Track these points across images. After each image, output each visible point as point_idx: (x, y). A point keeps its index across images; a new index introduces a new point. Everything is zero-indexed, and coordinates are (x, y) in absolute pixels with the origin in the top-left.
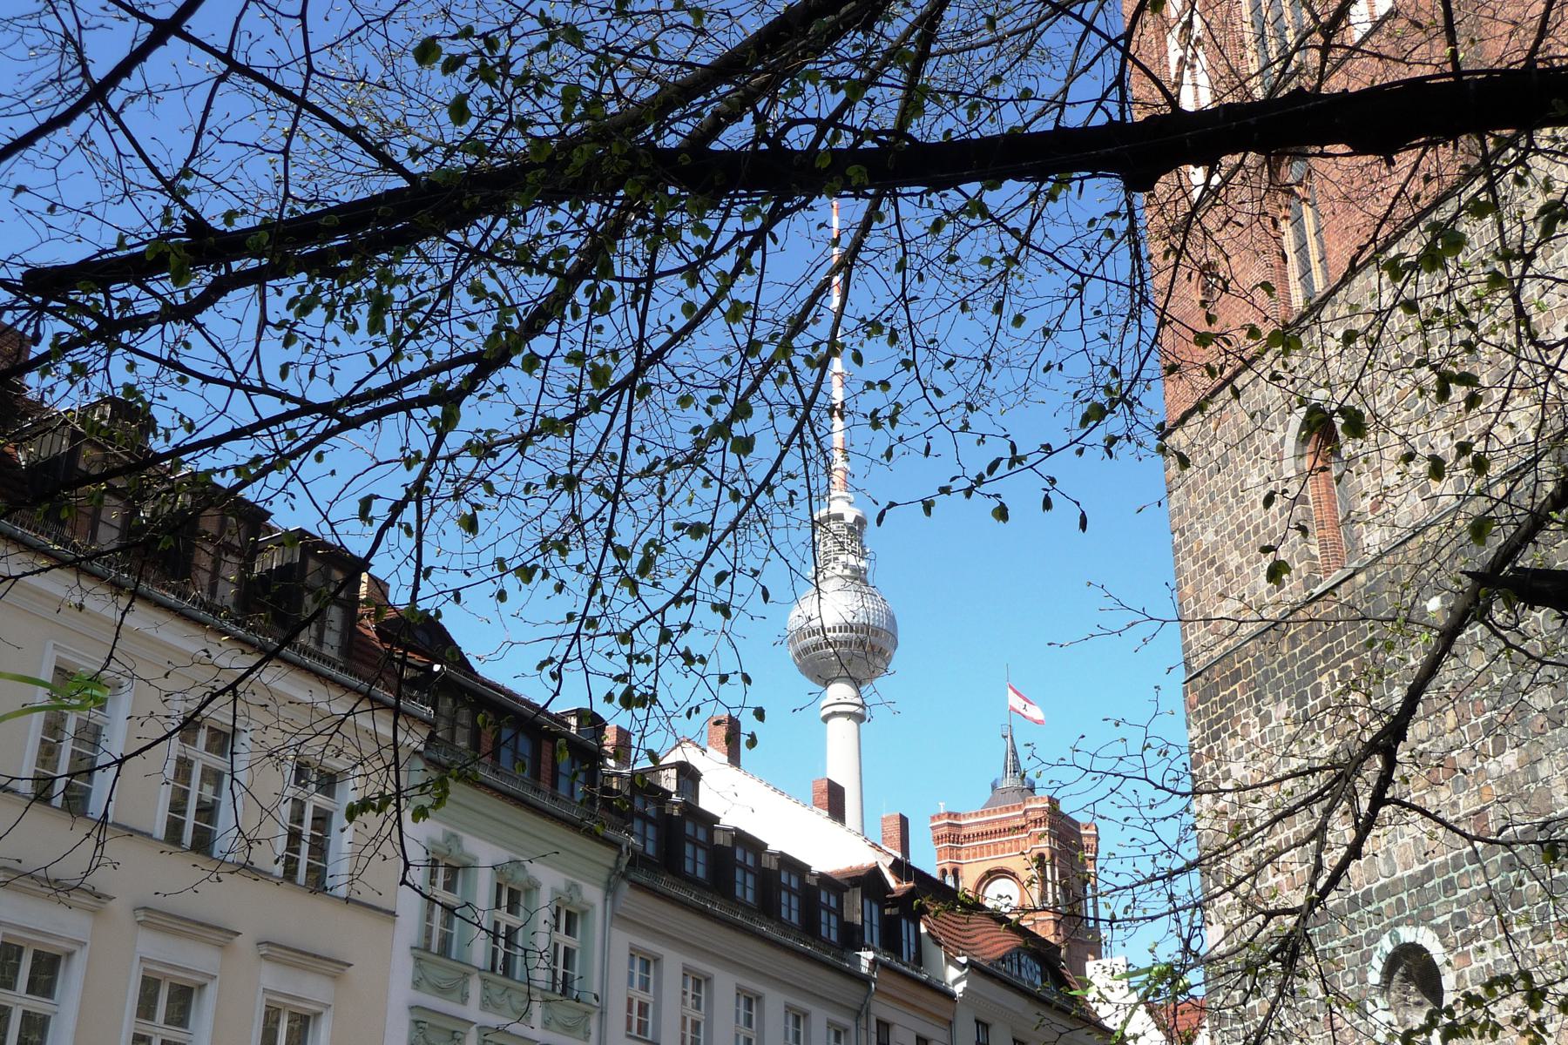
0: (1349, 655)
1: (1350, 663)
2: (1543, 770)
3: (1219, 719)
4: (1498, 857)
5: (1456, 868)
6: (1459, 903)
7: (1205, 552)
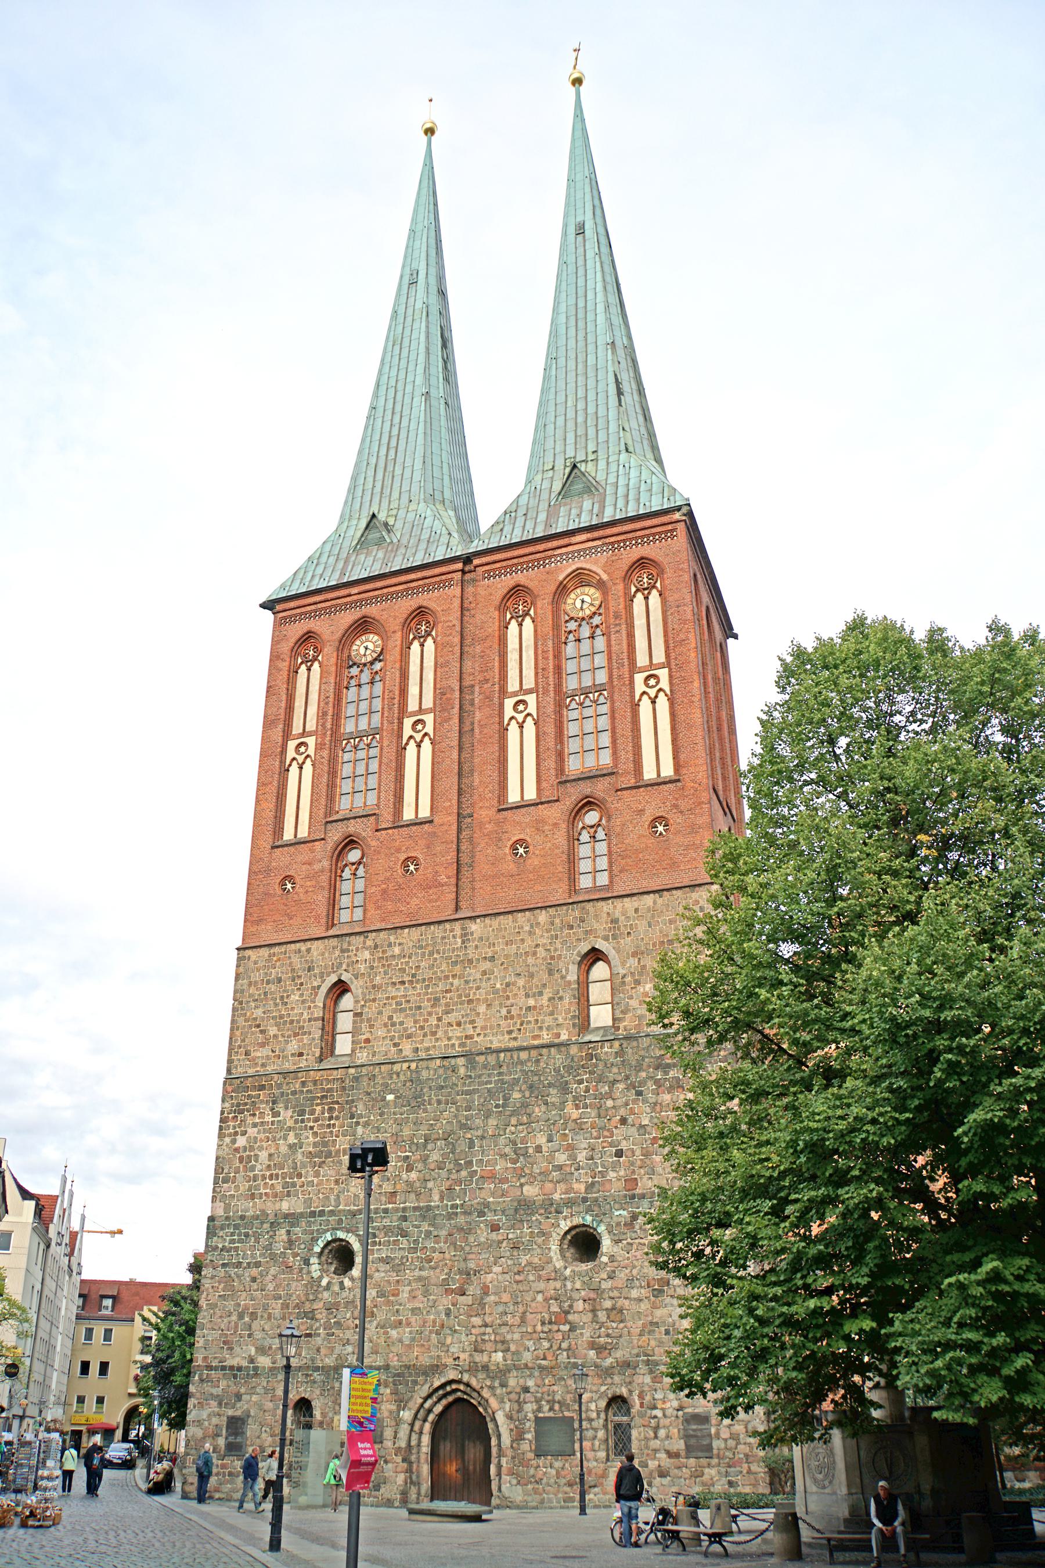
0: (337, 1103)
1: (336, 1106)
2: (430, 1185)
3: (246, 1104)
7: (255, 1019)
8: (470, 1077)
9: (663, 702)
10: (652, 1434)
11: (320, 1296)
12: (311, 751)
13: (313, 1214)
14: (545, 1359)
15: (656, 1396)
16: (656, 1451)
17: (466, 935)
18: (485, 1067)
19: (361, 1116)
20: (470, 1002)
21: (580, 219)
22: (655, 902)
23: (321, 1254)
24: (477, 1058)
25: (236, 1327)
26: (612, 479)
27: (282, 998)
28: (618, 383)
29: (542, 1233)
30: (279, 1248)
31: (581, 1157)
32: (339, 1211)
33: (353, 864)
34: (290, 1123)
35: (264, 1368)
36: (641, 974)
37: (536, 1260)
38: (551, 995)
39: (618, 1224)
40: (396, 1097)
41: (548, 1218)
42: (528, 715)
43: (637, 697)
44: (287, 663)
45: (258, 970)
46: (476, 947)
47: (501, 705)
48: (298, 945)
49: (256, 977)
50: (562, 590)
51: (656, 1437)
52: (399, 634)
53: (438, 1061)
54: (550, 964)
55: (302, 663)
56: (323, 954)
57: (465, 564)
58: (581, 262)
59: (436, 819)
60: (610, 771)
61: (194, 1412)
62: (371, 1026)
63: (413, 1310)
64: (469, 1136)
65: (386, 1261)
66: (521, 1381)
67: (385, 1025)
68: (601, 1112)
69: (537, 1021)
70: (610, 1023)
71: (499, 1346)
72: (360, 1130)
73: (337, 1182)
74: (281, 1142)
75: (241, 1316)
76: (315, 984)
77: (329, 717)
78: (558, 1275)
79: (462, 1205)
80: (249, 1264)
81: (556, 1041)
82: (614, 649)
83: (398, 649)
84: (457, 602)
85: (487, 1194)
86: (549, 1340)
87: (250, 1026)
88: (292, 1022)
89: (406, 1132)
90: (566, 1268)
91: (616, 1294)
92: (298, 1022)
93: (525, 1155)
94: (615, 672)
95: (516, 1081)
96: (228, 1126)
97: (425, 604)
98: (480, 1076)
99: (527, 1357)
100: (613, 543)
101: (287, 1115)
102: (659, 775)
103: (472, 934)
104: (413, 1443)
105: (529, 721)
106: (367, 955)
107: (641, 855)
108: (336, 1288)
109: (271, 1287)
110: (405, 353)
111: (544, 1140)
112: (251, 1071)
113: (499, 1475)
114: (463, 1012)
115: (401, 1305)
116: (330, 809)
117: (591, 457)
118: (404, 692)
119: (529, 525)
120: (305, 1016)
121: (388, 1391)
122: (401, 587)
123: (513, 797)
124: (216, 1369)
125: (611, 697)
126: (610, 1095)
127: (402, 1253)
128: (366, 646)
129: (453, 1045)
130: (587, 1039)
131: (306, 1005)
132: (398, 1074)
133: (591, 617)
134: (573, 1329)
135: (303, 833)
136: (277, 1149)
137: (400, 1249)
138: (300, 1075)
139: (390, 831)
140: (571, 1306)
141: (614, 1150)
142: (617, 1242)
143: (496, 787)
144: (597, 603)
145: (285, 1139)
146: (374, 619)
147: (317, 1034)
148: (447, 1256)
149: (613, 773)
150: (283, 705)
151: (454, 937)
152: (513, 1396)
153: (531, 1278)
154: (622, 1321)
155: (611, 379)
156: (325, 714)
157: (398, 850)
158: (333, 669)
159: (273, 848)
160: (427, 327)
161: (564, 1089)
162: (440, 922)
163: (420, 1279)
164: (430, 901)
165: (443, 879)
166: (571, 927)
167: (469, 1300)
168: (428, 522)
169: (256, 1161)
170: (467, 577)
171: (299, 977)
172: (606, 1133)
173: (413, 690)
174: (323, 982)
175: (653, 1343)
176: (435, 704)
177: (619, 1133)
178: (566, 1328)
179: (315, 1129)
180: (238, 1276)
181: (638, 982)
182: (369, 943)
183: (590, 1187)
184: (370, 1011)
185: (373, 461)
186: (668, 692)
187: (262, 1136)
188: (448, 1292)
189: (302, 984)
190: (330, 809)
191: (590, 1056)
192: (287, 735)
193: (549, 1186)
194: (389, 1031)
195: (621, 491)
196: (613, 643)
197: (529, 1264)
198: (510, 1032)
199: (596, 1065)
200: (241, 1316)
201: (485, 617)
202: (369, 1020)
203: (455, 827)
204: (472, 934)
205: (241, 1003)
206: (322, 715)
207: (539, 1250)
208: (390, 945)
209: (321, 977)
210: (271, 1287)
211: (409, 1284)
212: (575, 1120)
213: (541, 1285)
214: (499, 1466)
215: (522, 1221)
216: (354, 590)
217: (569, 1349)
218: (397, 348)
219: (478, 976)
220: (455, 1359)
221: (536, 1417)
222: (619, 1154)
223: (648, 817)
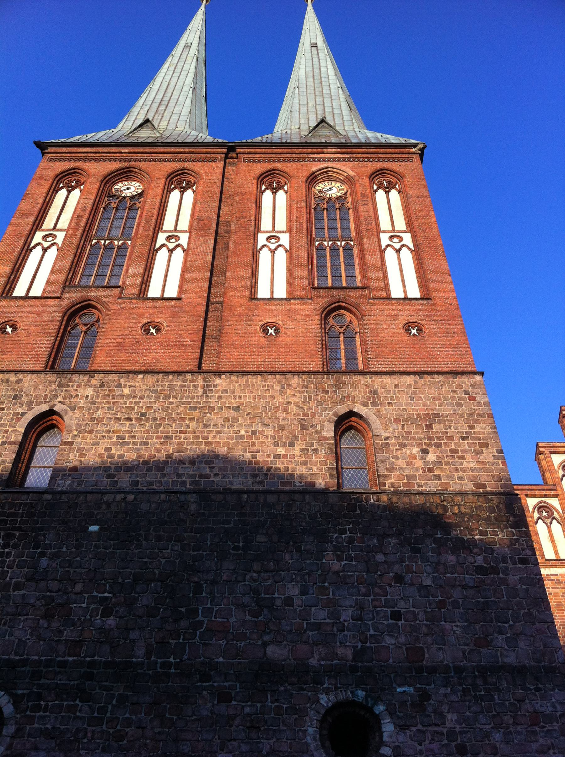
0: (19, 529)
2: (134, 635)
4: (82, 670)
8: (203, 514)
19: (49, 546)
22: (415, 381)
24: (213, 497)
31: (346, 615)
38: (304, 447)
40: (100, 529)
41: (303, 690)
46: (220, 397)
48: (7, 376)
50: (312, 179)
52: (162, 181)
53: (163, 496)
54: (302, 419)
56: (36, 386)
59: (184, 298)
64: (196, 579)
72: (44, 562)
76: (20, 411)
77: (84, 220)
94: (364, 228)
103: (216, 386)
105: (281, 251)
107: (396, 347)
111: (296, 591)
128: (130, 188)
129: (184, 483)
137: (76, 718)
139: (134, 301)
141: (389, 610)
157: (141, 315)
164: (170, 357)
166: (327, 392)
172: (377, 590)
174: (30, 409)
176: (191, 226)
181: (403, 445)
182: (93, 382)
183: (359, 654)
204: (216, 386)
208: (119, 386)
212: (337, 573)
216: (126, 150)
219: (220, 422)
222: (396, 616)
223: (402, 319)
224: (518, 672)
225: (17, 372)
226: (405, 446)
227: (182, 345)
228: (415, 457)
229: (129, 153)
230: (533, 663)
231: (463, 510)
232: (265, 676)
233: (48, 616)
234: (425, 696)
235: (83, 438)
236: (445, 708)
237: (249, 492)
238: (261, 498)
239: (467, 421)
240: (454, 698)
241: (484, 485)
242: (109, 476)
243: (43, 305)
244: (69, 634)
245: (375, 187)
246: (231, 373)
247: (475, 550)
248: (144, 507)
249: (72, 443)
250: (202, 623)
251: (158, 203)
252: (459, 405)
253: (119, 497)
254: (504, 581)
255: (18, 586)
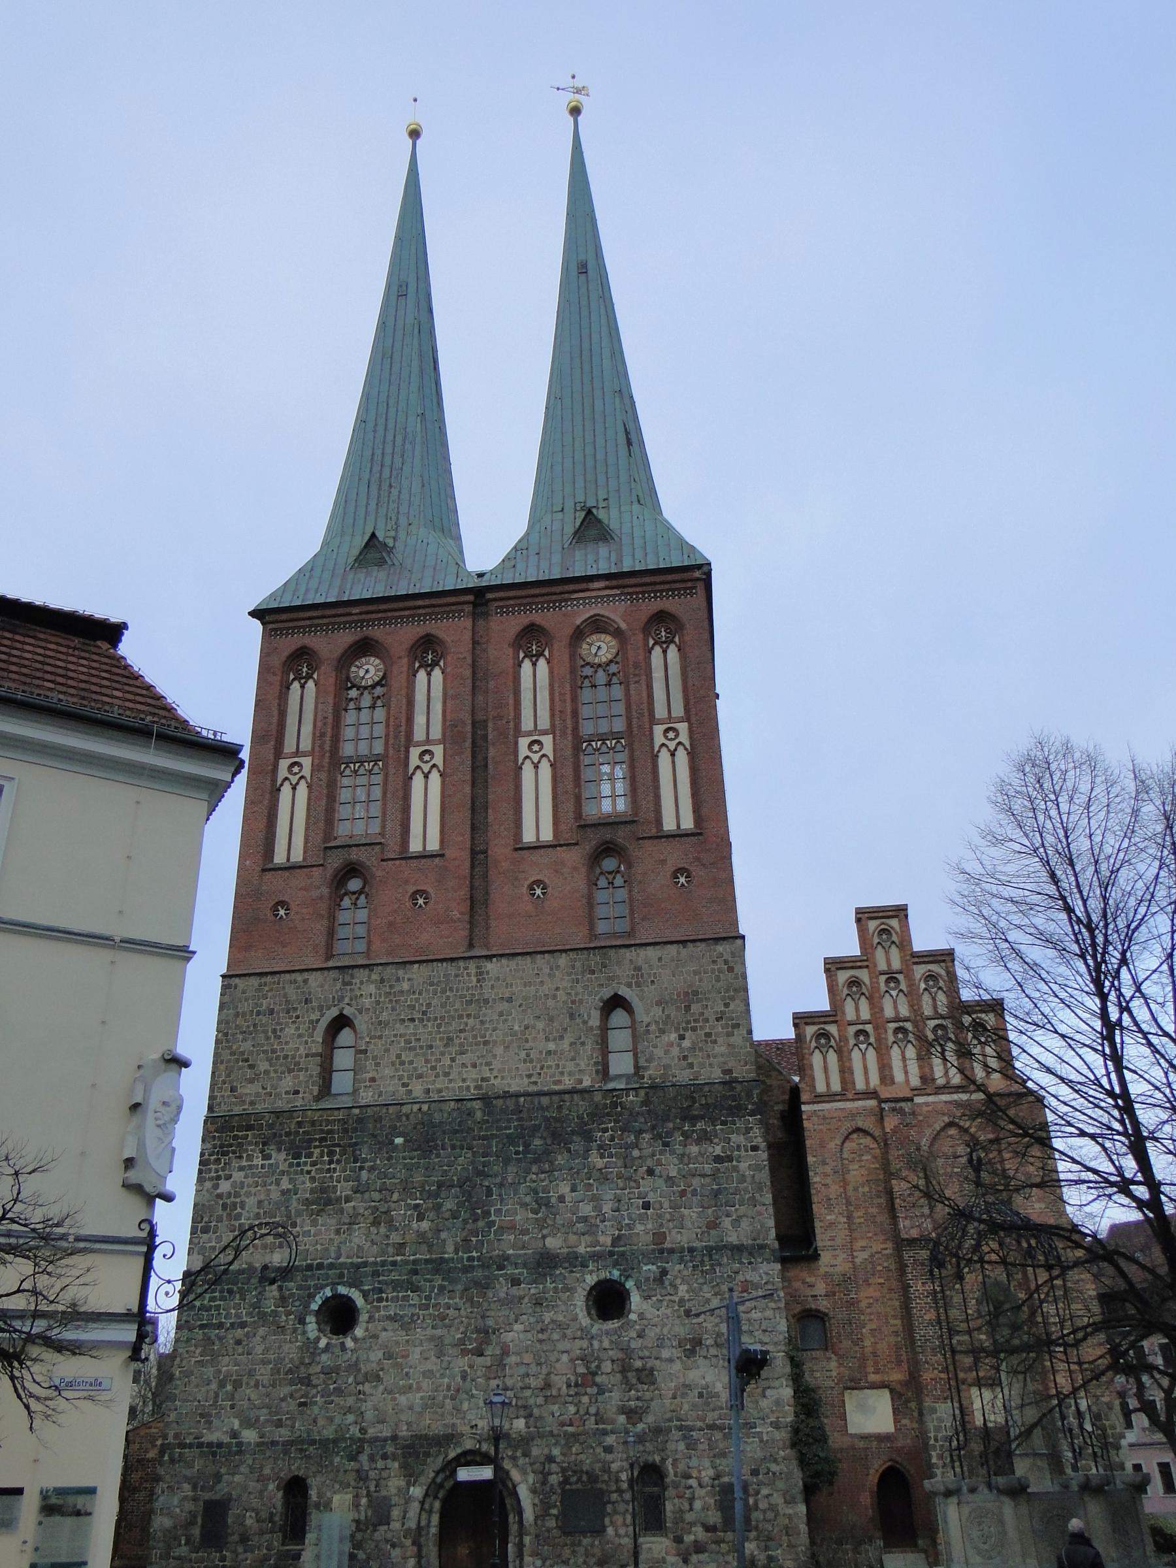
0: (339, 1145)
2: (443, 1235)
5: (383, 1266)
6: (379, 1282)
7: (243, 1053)
8: (487, 1121)
9: (682, 757)
10: (686, 1506)
11: (317, 1359)
12: (307, 771)
13: (309, 1267)
14: (571, 1425)
15: (691, 1465)
16: (692, 1524)
17: (481, 973)
18: (503, 1111)
19: (365, 1160)
20: (486, 1043)
21: (582, 257)
22: (679, 953)
23: (318, 1313)
25: (216, 1395)
26: (626, 528)
27: (274, 1031)
28: (627, 433)
29: (566, 1289)
30: (270, 1306)
31: (607, 1208)
32: (341, 1264)
33: (354, 893)
34: (283, 1167)
35: (249, 1443)
36: (665, 1023)
37: (560, 1318)
39: (647, 1279)
42: (544, 755)
43: (656, 749)
44: (279, 678)
45: (246, 1000)
47: (516, 743)
48: (294, 976)
49: (245, 1007)
50: (578, 635)
51: (691, 1509)
52: (405, 660)
53: (452, 1103)
55: (294, 679)
57: (476, 597)
58: (584, 303)
59: (447, 852)
60: (630, 819)
61: (161, 1498)
62: (377, 1065)
63: (424, 1373)
65: (393, 1319)
66: (546, 1451)
67: (393, 1064)
68: (627, 1162)
69: (558, 1066)
70: (632, 1071)
71: (522, 1412)
73: (338, 1232)
74: (273, 1187)
75: (222, 1385)
76: (314, 1017)
78: (585, 1334)
79: (479, 1259)
80: (232, 1324)
81: (579, 1087)
82: (633, 698)
83: (404, 676)
84: (468, 635)
85: (508, 1245)
86: (576, 1405)
87: (237, 1061)
88: (286, 1057)
89: (418, 1178)
90: (592, 1326)
91: (646, 1353)
92: (294, 1057)
93: (547, 1205)
94: (635, 721)
95: (536, 1128)
96: (210, 1170)
97: (433, 632)
98: (498, 1121)
99: (551, 1425)
100: (631, 594)
101: (279, 1158)
102: (678, 826)
104: (423, 1523)
106: (372, 988)
108: (337, 1350)
109: (259, 1349)
110: (396, 369)
112: (237, 1110)
113: (520, 1555)
114: (478, 1053)
115: (411, 1367)
116: (328, 835)
117: (602, 504)
118: (410, 720)
119: (544, 565)
120: (302, 1051)
121: (396, 1465)
122: (407, 613)
123: (528, 837)
124: (191, 1446)
125: (630, 745)
126: (636, 1145)
127: (412, 1310)
129: (468, 1088)
130: (611, 1086)
131: (301, 1039)
132: (407, 1116)
133: (608, 665)
134: (601, 1392)
135: (297, 856)
136: (268, 1195)
138: (295, 1114)
139: (397, 862)
140: (598, 1367)
141: (641, 1201)
142: (647, 1298)
143: (512, 825)
144: (614, 651)
145: (278, 1184)
146: (377, 642)
147: (315, 1070)
148: (463, 1312)
149: (634, 822)
150: (275, 720)
151: (469, 975)
152: (537, 1466)
153: (555, 1336)
154: (653, 1383)
155: (621, 428)
156: (323, 735)
157: (406, 882)
158: (332, 689)
159: (264, 870)
160: (420, 345)
161: (588, 1137)
162: (452, 960)
163: (432, 1339)
164: (441, 937)
165: (456, 914)
166: (593, 972)
167: (487, 1361)
168: (432, 548)
169: (242, 1208)
170: (479, 610)
171: (295, 1009)
172: (633, 1184)
173: (420, 720)
174: (322, 1015)
175: (686, 1407)
177: (646, 1184)
178: (593, 1390)
179: (313, 1174)
180: (220, 1339)
182: (374, 977)
183: (616, 1241)
184: (376, 1048)
185: (366, 477)
186: (688, 747)
187: (250, 1180)
188: (465, 1352)
189: (297, 1017)
190: (328, 835)
191: (614, 1105)
192: (278, 754)
193: (573, 1238)
194: (397, 1070)
195: (638, 542)
196: (632, 692)
197: (553, 1321)
198: (529, 1076)
199: (620, 1114)
200: (222, 1385)
201: (499, 652)
202: (375, 1058)
203: (467, 863)
204: (488, 973)
205: (226, 1034)
206: (318, 736)
207: (563, 1308)
208: (398, 980)
209: (321, 1008)
210: (259, 1349)
211: (421, 1345)
212: (600, 1170)
213: (564, 1345)
214: (520, 1546)
215: (545, 1275)
216: (356, 610)
217: (596, 1415)
218: (387, 362)
220: (472, 1427)
221: (563, 1490)
222: (647, 1206)
223: (670, 868)
224: (738, 1249)
225: (301, 971)
226: (664, 1032)
227: (452, 919)
228: (672, 1045)
229: (361, 613)
230: (750, 1242)
231: (710, 1101)
232: (545, 1263)
233: (376, 1223)
234: (664, 1272)
235: (375, 1044)
236: (678, 1281)
237: (527, 1094)
238: (536, 1100)
239: (723, 998)
240: (685, 1273)
241: (730, 1071)
242: (404, 1085)
243: (310, 877)
244: (395, 1238)
245: (651, 642)
246: (502, 956)
247: (716, 1140)
248: (437, 1117)
249: (365, 1052)
250: (494, 1222)
251: (404, 701)
252: (718, 980)
253: (416, 1107)
254: (736, 1169)
255: (348, 1200)
